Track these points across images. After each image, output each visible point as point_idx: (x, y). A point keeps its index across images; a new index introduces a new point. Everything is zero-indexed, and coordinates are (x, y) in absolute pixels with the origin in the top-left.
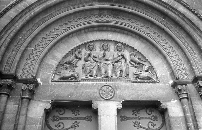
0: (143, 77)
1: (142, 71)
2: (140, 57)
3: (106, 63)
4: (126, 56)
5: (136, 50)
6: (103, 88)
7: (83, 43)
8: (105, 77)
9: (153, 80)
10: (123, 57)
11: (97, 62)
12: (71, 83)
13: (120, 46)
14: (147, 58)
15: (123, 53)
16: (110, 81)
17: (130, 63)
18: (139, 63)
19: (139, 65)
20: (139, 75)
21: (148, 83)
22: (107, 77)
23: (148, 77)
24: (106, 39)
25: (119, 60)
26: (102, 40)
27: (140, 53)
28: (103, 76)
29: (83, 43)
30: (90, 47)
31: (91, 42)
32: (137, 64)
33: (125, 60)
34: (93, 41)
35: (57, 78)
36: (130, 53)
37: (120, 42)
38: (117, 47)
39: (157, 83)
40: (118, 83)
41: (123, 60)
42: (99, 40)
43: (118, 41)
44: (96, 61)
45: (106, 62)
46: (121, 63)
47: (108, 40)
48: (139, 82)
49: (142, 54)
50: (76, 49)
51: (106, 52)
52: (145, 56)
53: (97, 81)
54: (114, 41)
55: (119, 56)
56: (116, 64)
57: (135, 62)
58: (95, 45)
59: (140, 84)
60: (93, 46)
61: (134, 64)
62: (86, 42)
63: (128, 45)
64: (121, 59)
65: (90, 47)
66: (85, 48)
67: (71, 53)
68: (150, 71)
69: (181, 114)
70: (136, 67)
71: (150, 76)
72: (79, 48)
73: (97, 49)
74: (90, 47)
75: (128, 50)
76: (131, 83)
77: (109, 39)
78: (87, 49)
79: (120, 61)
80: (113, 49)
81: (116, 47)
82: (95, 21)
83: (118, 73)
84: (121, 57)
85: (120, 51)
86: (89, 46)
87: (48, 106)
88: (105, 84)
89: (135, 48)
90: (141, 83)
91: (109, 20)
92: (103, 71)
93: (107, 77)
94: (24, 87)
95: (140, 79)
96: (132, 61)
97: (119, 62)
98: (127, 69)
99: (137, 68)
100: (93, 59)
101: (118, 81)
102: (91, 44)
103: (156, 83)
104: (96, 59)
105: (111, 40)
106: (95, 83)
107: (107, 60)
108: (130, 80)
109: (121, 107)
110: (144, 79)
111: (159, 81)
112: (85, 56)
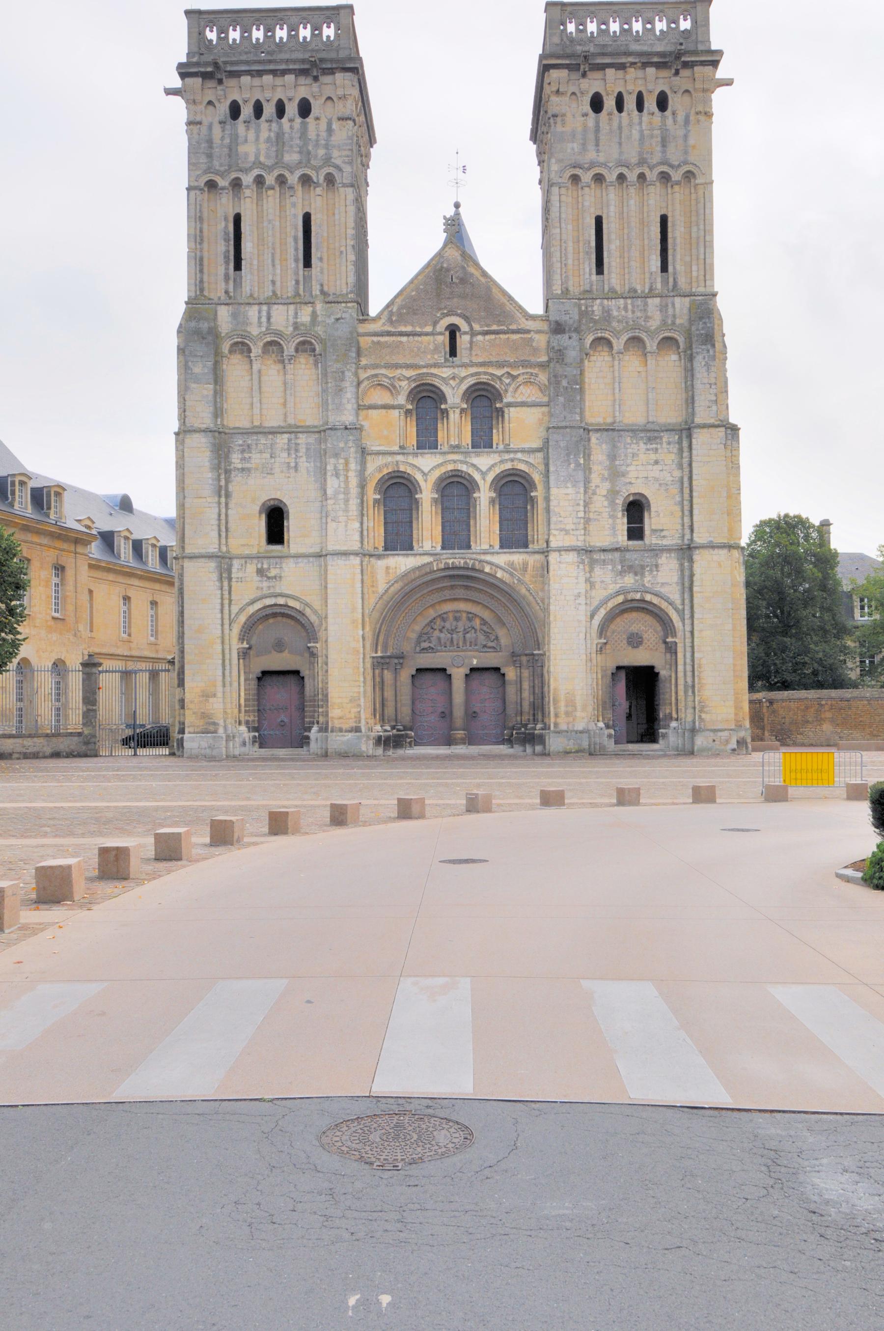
35: (418, 649)
41: (473, 631)
50: (431, 622)
67: (428, 625)
69: (515, 678)
82: (447, 594)
83: (468, 644)
86: (443, 617)
87: (414, 672)
91: (460, 593)
92: (455, 643)
94: (396, 661)
98: (476, 639)
102: (445, 616)
108: (477, 651)
109: (468, 672)
110: (490, 647)
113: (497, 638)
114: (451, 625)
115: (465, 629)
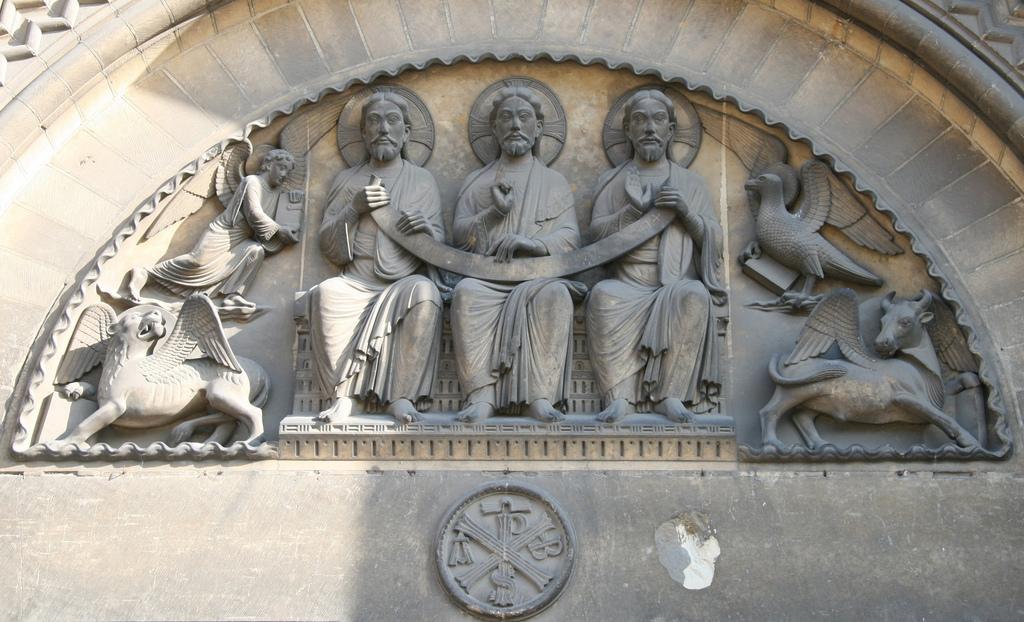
0: (861, 407)
1: (845, 350)
2: (845, 212)
3: (515, 283)
4: (714, 204)
5: (805, 143)
6: (472, 512)
7: (312, 97)
8: (498, 412)
9: (955, 439)
10: (680, 219)
11: (437, 269)
12: (189, 471)
13: (656, 117)
14: (903, 225)
15: (673, 184)
16: (535, 449)
17: (747, 273)
18: (834, 275)
19: (827, 292)
20: (814, 389)
21: (894, 467)
22: (521, 409)
23: (895, 403)
24: (528, 53)
25: (640, 247)
26: (489, 60)
27: (844, 178)
28: (483, 402)
29: (307, 92)
30: (371, 135)
31: (382, 80)
32: (810, 281)
33: (698, 249)
34: (409, 71)
36: (752, 173)
37: (653, 80)
38: (626, 120)
39: (981, 466)
40: (610, 466)
41: (676, 246)
42: (462, 63)
43: (641, 65)
44: (422, 267)
45: (515, 269)
46: (658, 272)
47: (544, 60)
48: (811, 458)
49: (862, 184)
51: (515, 175)
52: (883, 204)
53: (423, 449)
54: (599, 65)
55: (637, 212)
56: (606, 287)
57: (795, 266)
58: (423, 107)
59: (816, 472)
60: (407, 121)
61: (782, 280)
62: (337, 80)
63: (731, 102)
64: (661, 235)
65: (375, 128)
66: (332, 135)
68: (924, 351)
70: (798, 310)
71: (923, 400)
72: (278, 146)
73: (442, 142)
74: (375, 128)
75: (730, 148)
76: (732, 467)
77: (557, 52)
78: (355, 153)
79: (646, 255)
80: (597, 138)
81: (620, 117)
83: (622, 373)
84: (646, 226)
85: (649, 162)
88: (497, 482)
89: (796, 132)
90: (828, 467)
92: (478, 356)
93: (521, 409)
95: (826, 420)
96: (764, 250)
97: (636, 271)
99: (801, 322)
100: (398, 246)
101: (611, 449)
102: (385, 101)
103: (972, 466)
104: (421, 246)
105: (572, 62)
106: (409, 466)
107: (522, 252)
110: (861, 422)
111: (1006, 448)
112: (330, 220)
113: (941, 310)
114: (450, 207)
115: (589, 236)
